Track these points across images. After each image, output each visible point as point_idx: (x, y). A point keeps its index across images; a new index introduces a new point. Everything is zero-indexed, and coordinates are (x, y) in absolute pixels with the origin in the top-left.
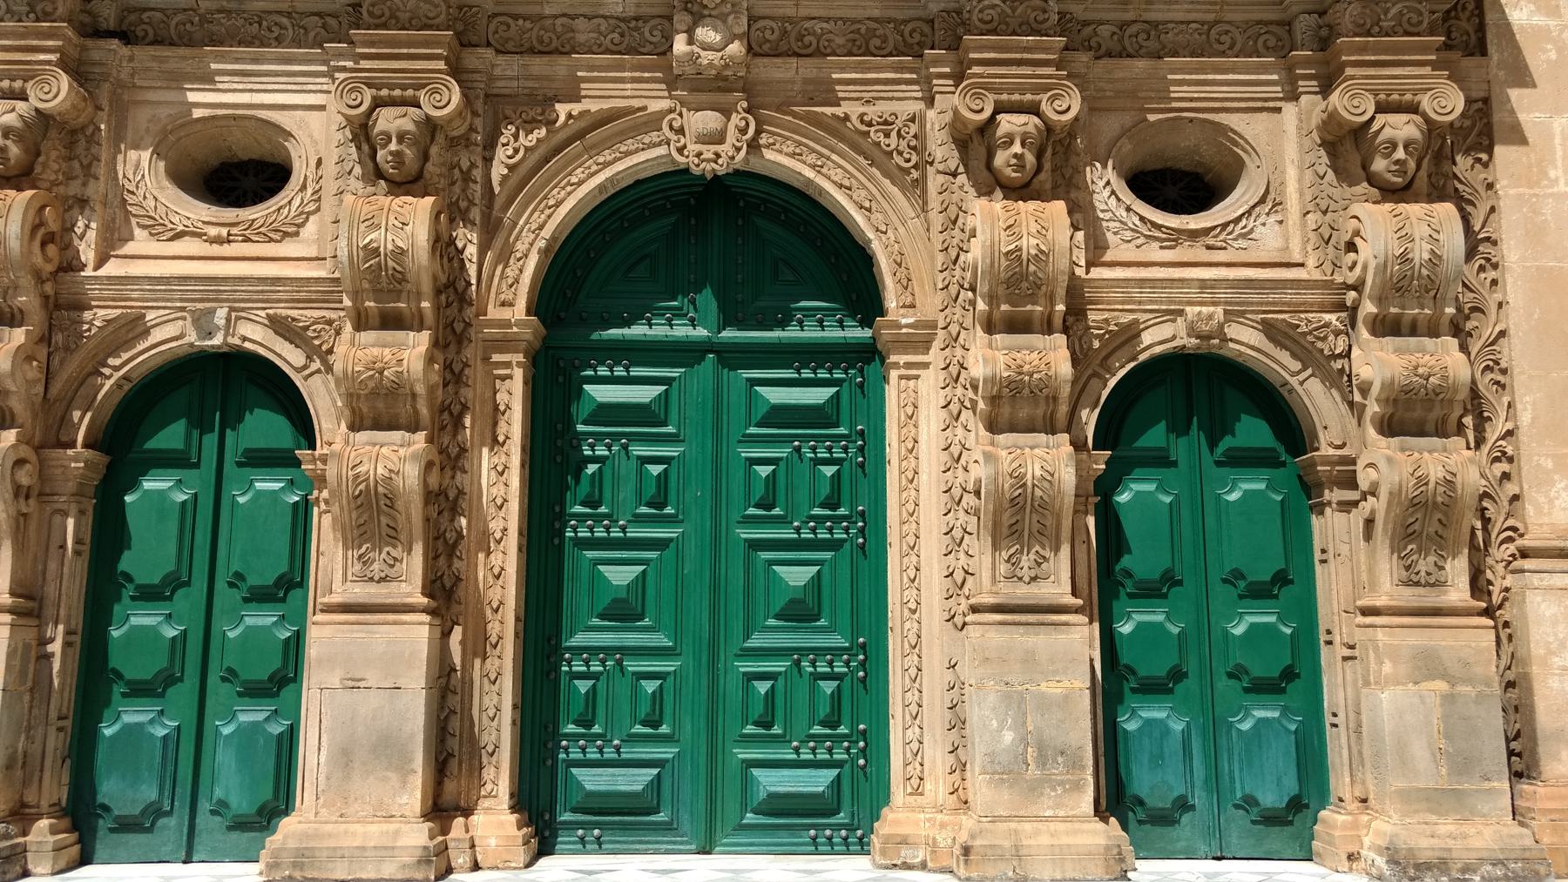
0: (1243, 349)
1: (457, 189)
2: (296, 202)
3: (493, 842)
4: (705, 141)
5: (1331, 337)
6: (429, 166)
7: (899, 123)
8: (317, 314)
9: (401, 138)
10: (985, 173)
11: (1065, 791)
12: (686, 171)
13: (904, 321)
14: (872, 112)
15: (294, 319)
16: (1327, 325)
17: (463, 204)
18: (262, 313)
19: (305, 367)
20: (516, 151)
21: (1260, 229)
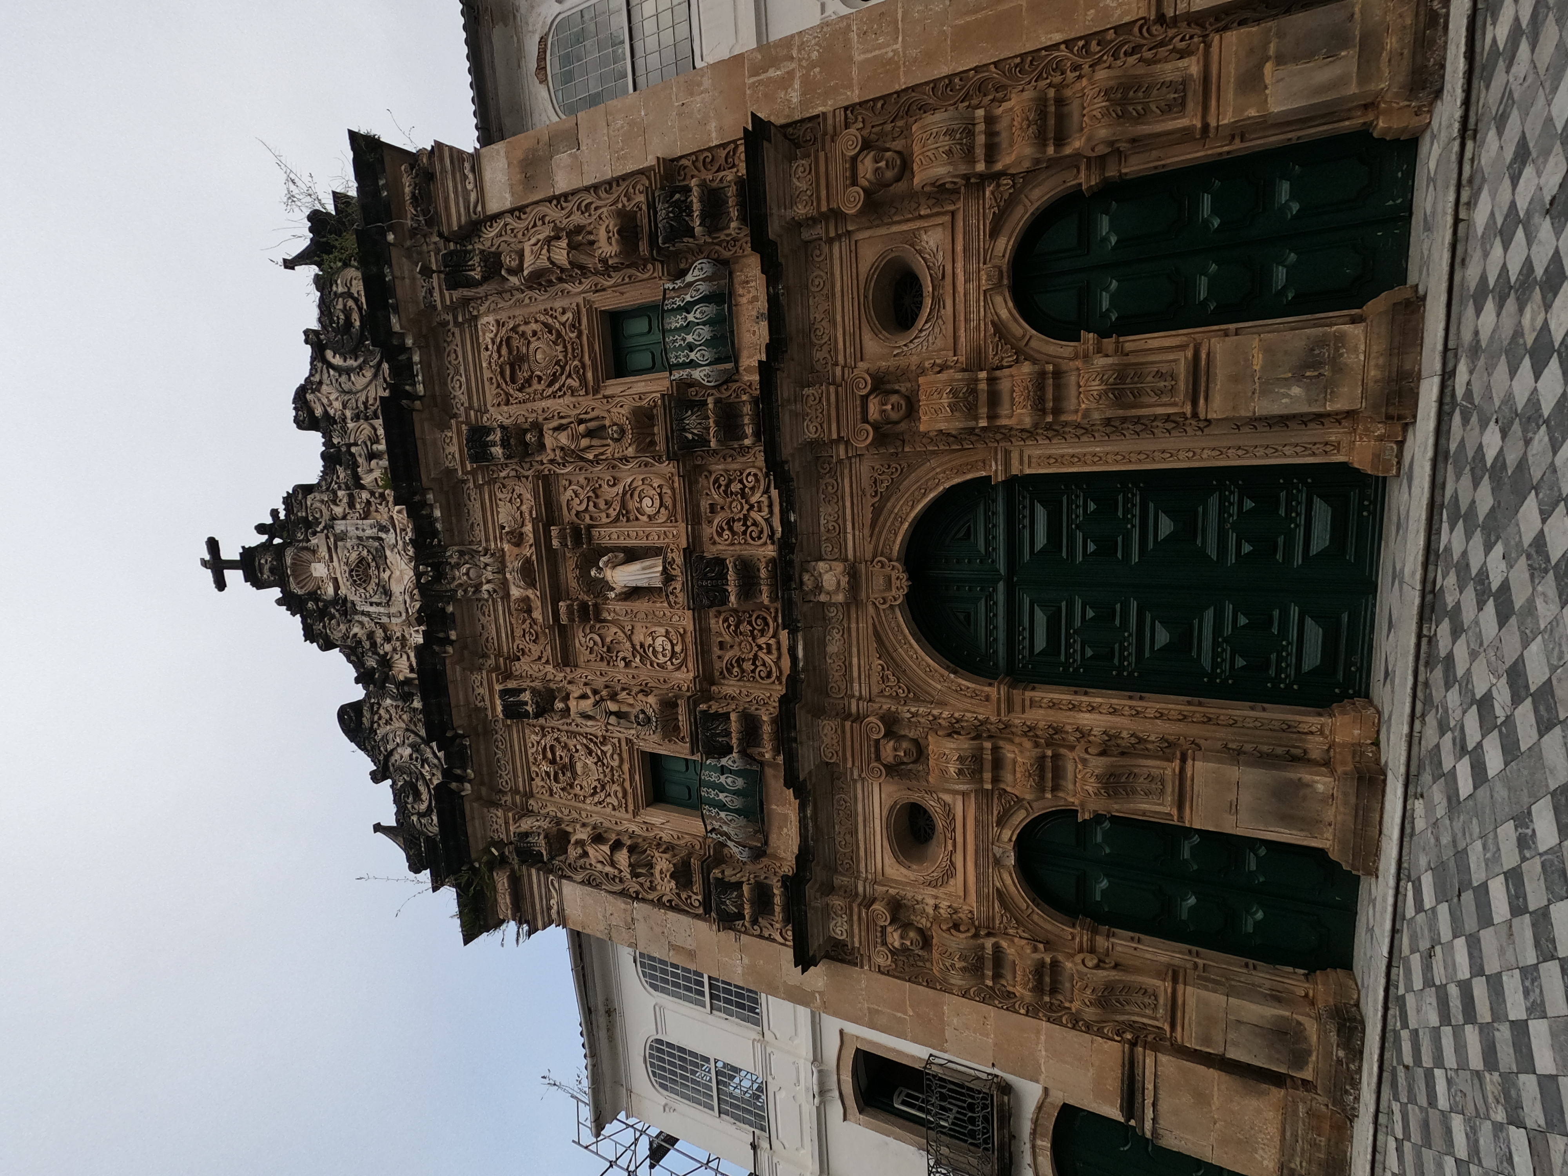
0: (1010, 247)
1: (922, 720)
2: (932, 803)
3: (1357, 732)
4: (890, 584)
5: (1002, 189)
7: (876, 475)
10: (902, 424)
11: (1343, 346)
12: (907, 596)
13: (994, 468)
14: (869, 491)
16: (993, 193)
19: (1026, 809)
21: (931, 243)
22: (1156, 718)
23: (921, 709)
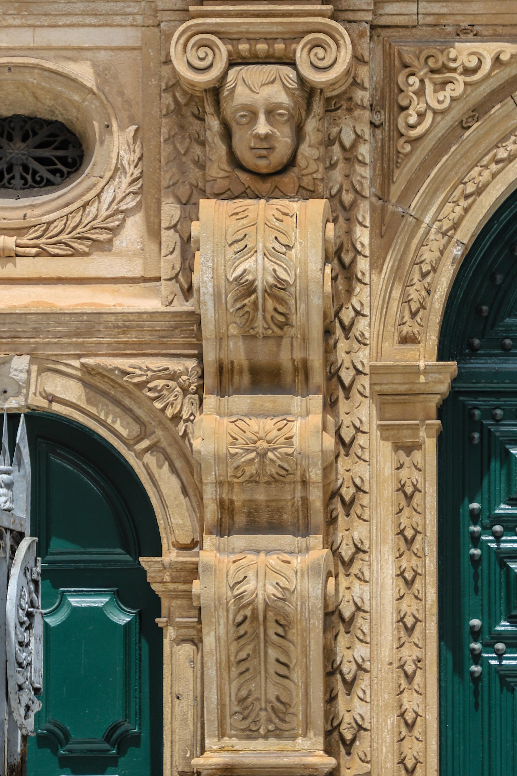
1: (337, 175)
6: (305, 149)
8: (156, 364)
9: (271, 113)
15: (125, 373)
17: (347, 198)
18: (76, 363)
20: (421, 116)
23: (366, 172)
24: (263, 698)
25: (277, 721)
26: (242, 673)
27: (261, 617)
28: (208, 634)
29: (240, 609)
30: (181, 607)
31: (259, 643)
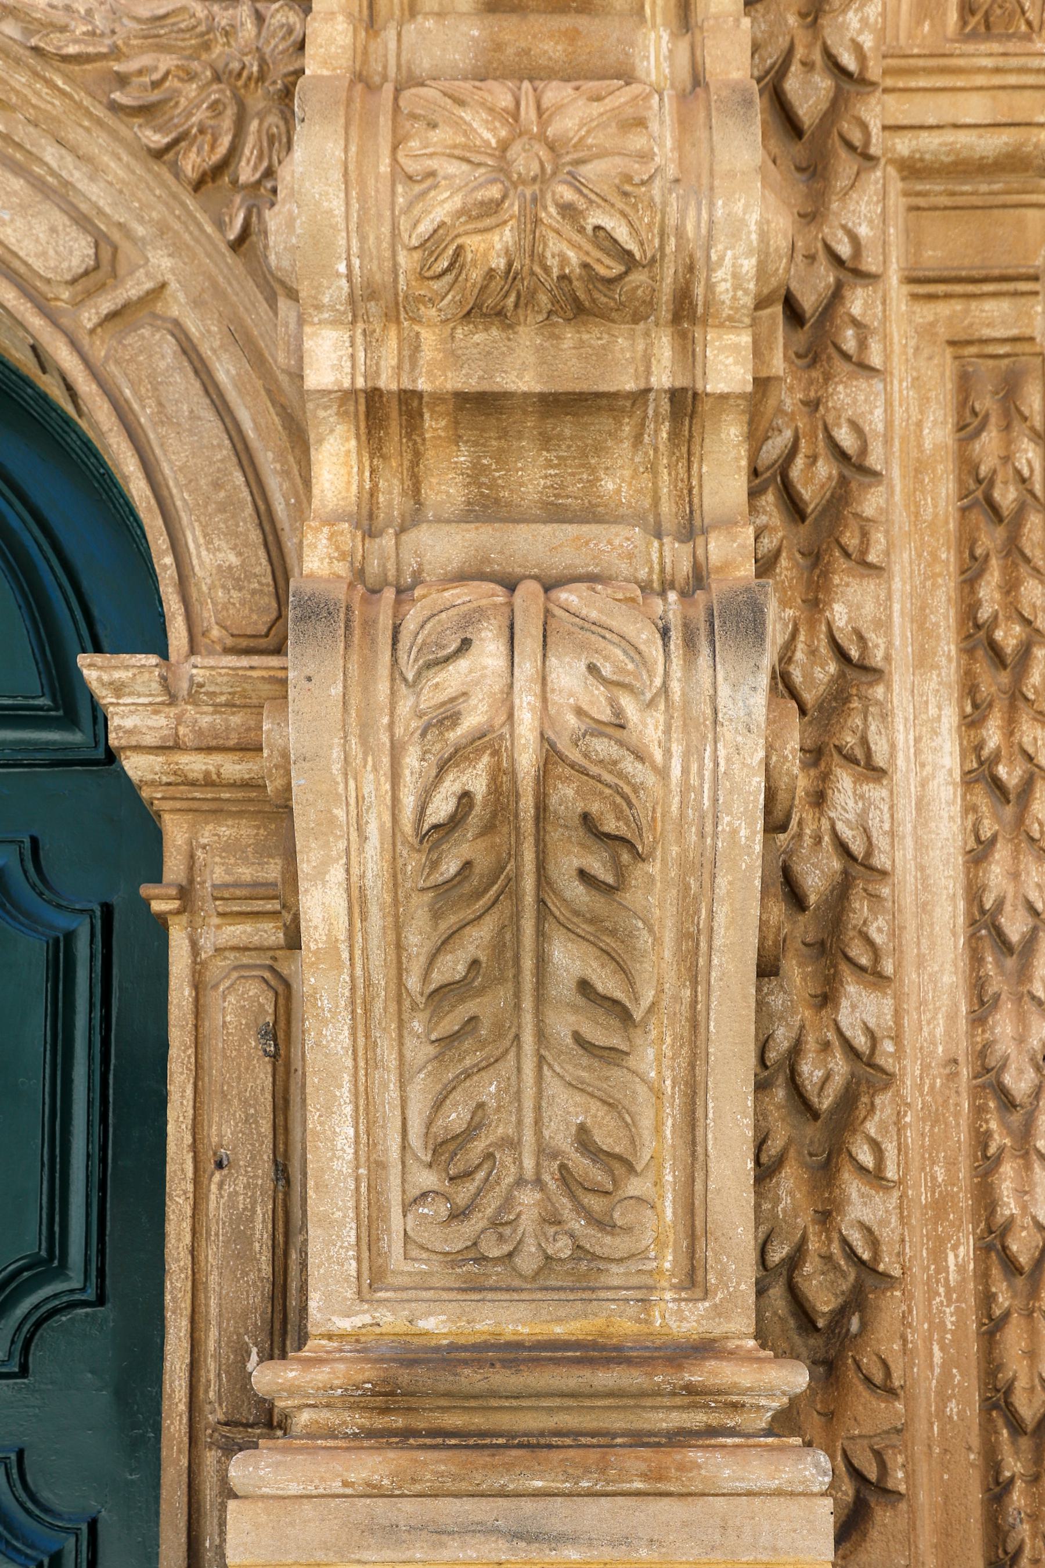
22: (993, 1242)
24: (528, 1137)
25: (578, 1225)
26: (449, 1041)
27: (527, 803)
28: (320, 874)
29: (442, 769)
30: (231, 848)
31: (516, 917)
